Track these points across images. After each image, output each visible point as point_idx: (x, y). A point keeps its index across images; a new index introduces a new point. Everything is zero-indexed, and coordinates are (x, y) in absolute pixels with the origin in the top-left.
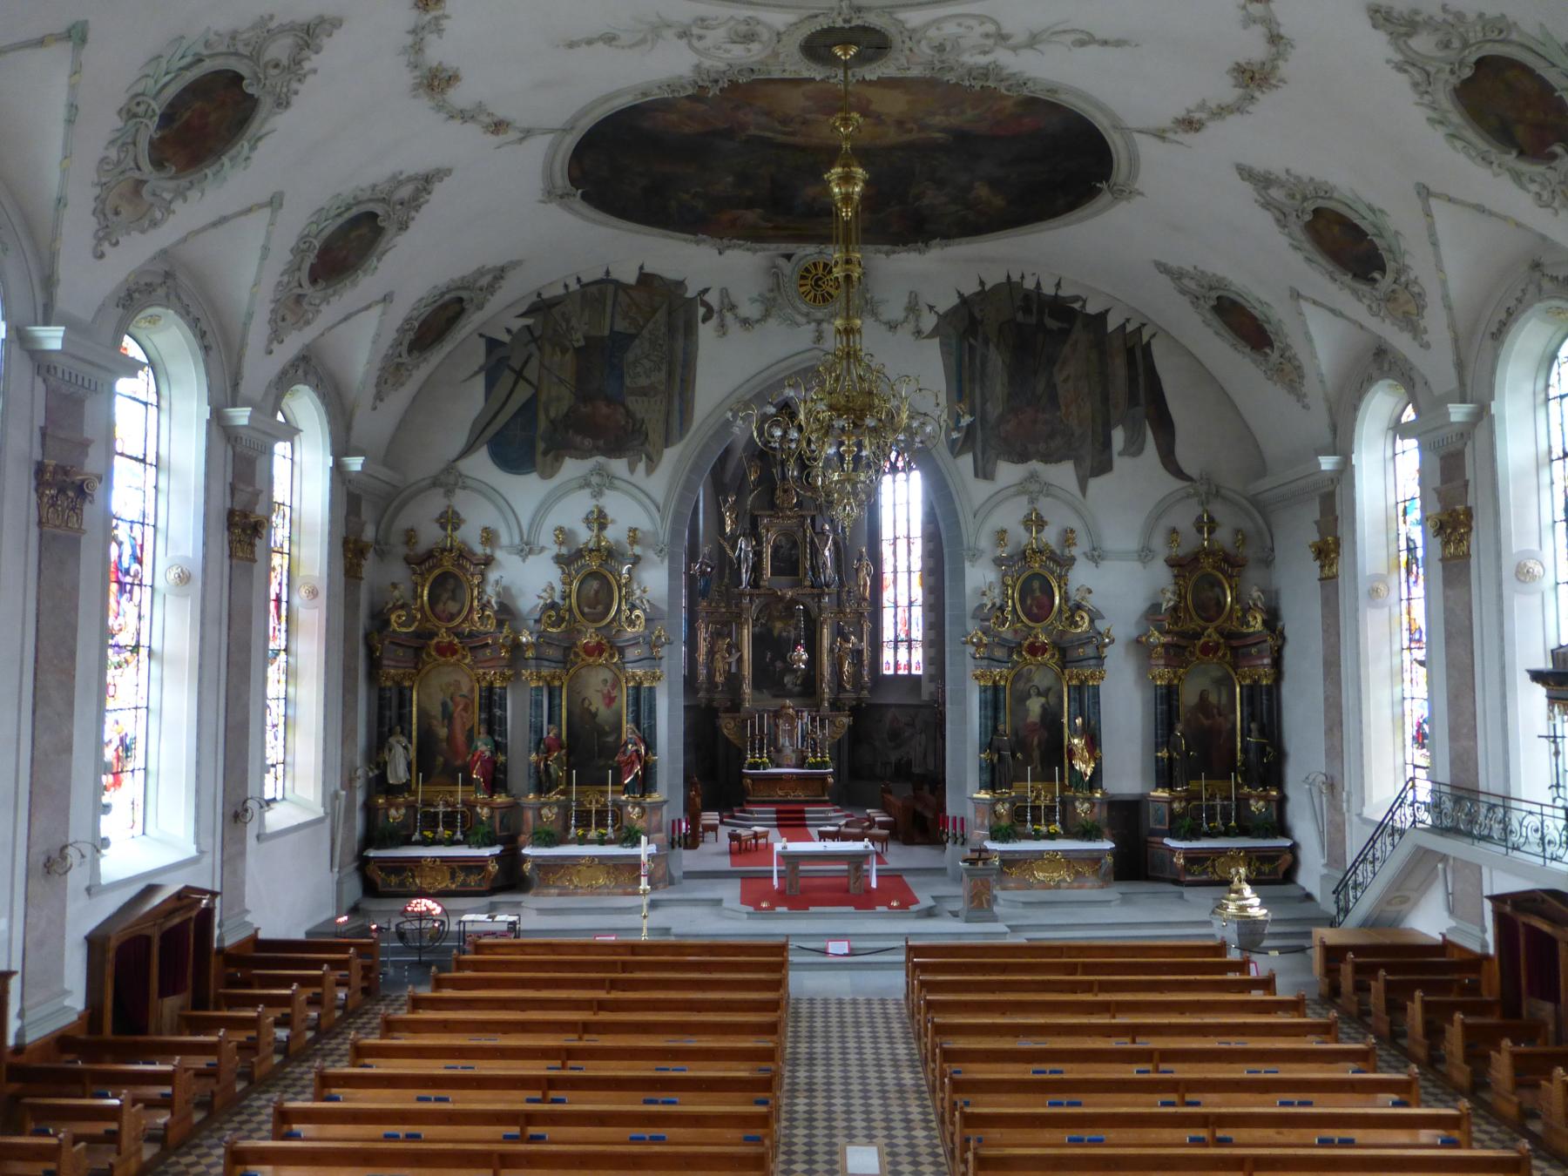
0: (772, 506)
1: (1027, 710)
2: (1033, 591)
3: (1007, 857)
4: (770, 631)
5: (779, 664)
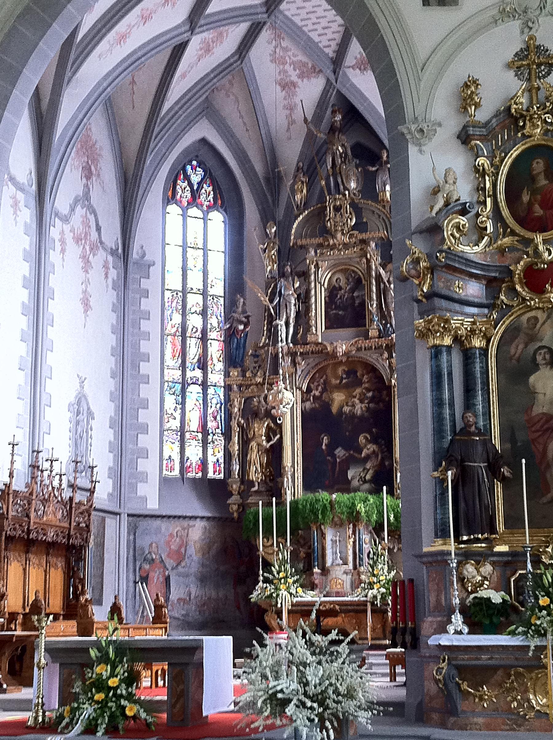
0: (326, 232)
1: (532, 394)
2: (533, 179)
3: (464, 659)
4: (327, 406)
5: (340, 452)
